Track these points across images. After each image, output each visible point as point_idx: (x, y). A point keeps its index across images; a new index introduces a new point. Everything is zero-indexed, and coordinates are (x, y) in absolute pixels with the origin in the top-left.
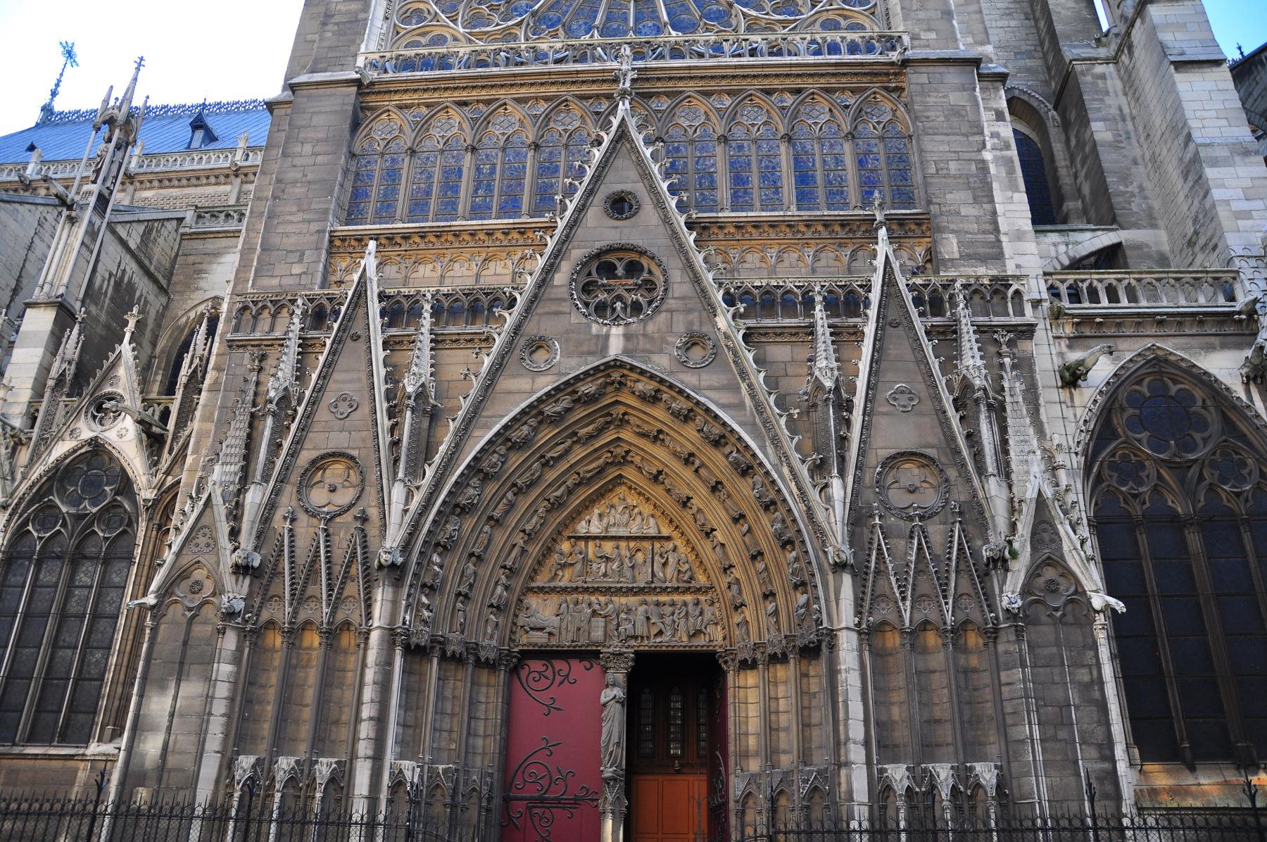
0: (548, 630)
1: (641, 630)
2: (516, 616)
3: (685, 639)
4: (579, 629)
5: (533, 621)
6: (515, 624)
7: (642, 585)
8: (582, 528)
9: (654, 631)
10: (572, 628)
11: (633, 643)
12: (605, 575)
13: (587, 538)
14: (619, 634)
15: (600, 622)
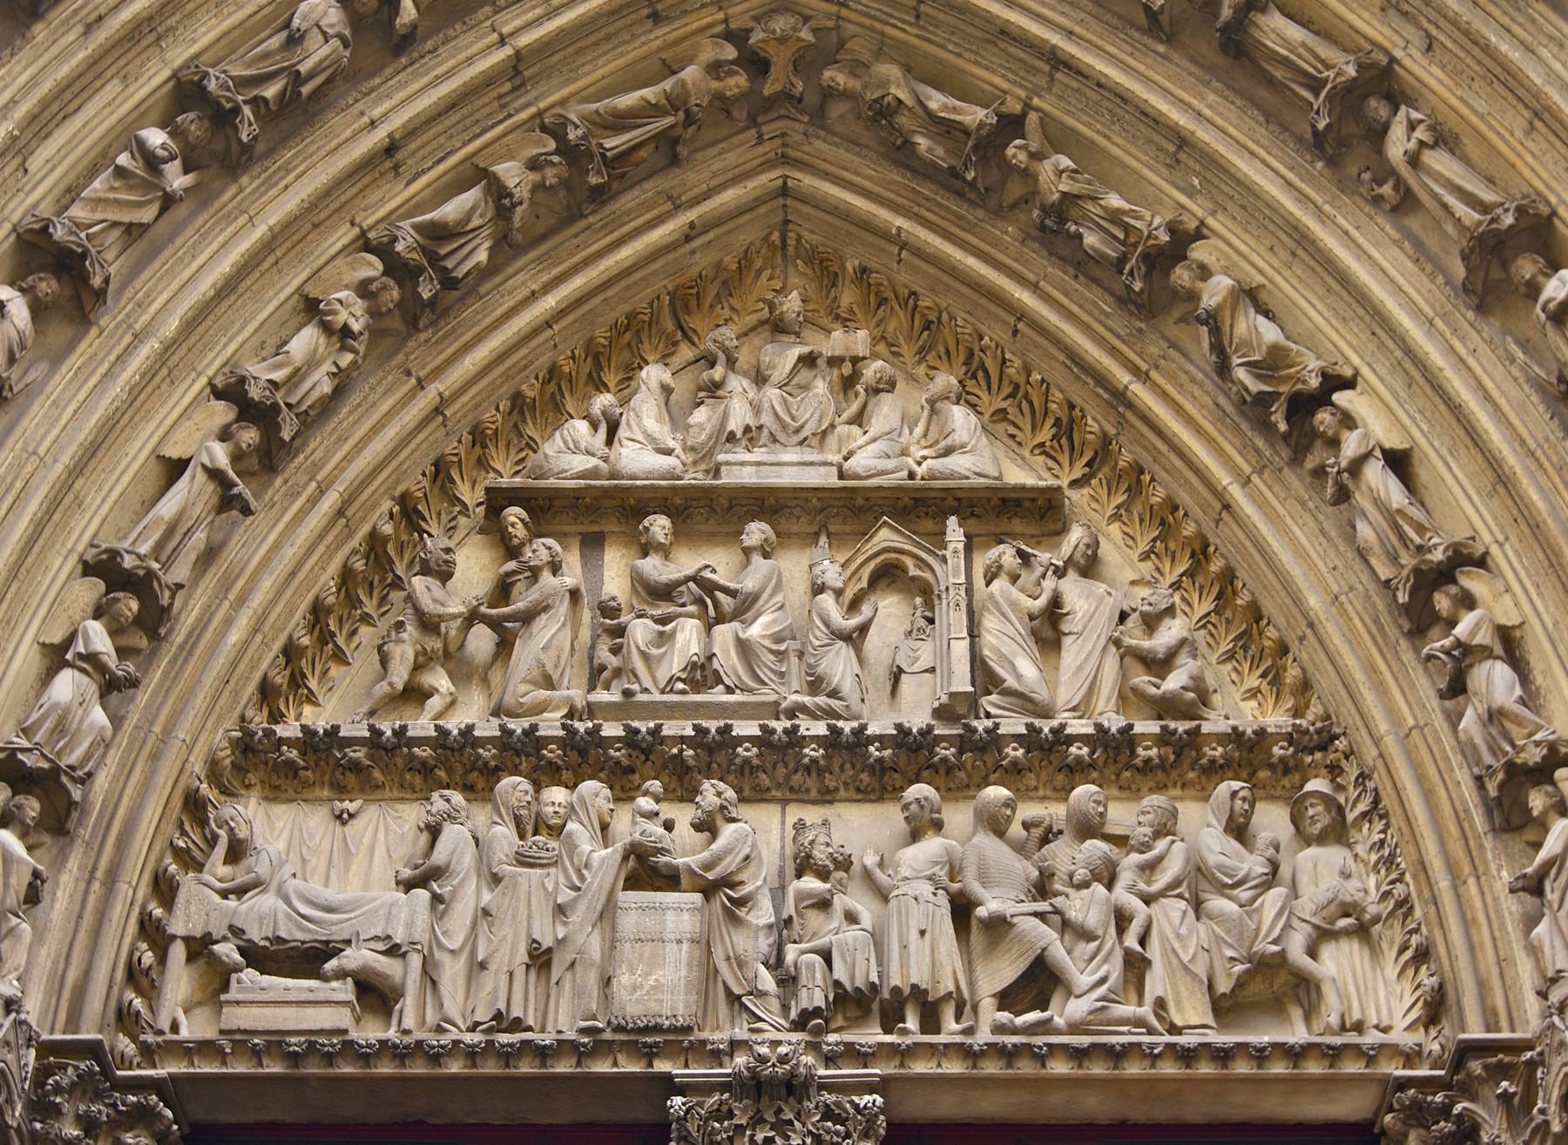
0: (357, 957)
1: (926, 954)
2: (165, 889)
3: (1192, 1011)
4: (540, 959)
5: (263, 915)
6: (153, 933)
7: (918, 719)
8: (569, 453)
9: (1004, 971)
10: (508, 951)
11: (872, 1035)
12: (701, 674)
13: (604, 512)
14: (789, 982)
15: (678, 912)
